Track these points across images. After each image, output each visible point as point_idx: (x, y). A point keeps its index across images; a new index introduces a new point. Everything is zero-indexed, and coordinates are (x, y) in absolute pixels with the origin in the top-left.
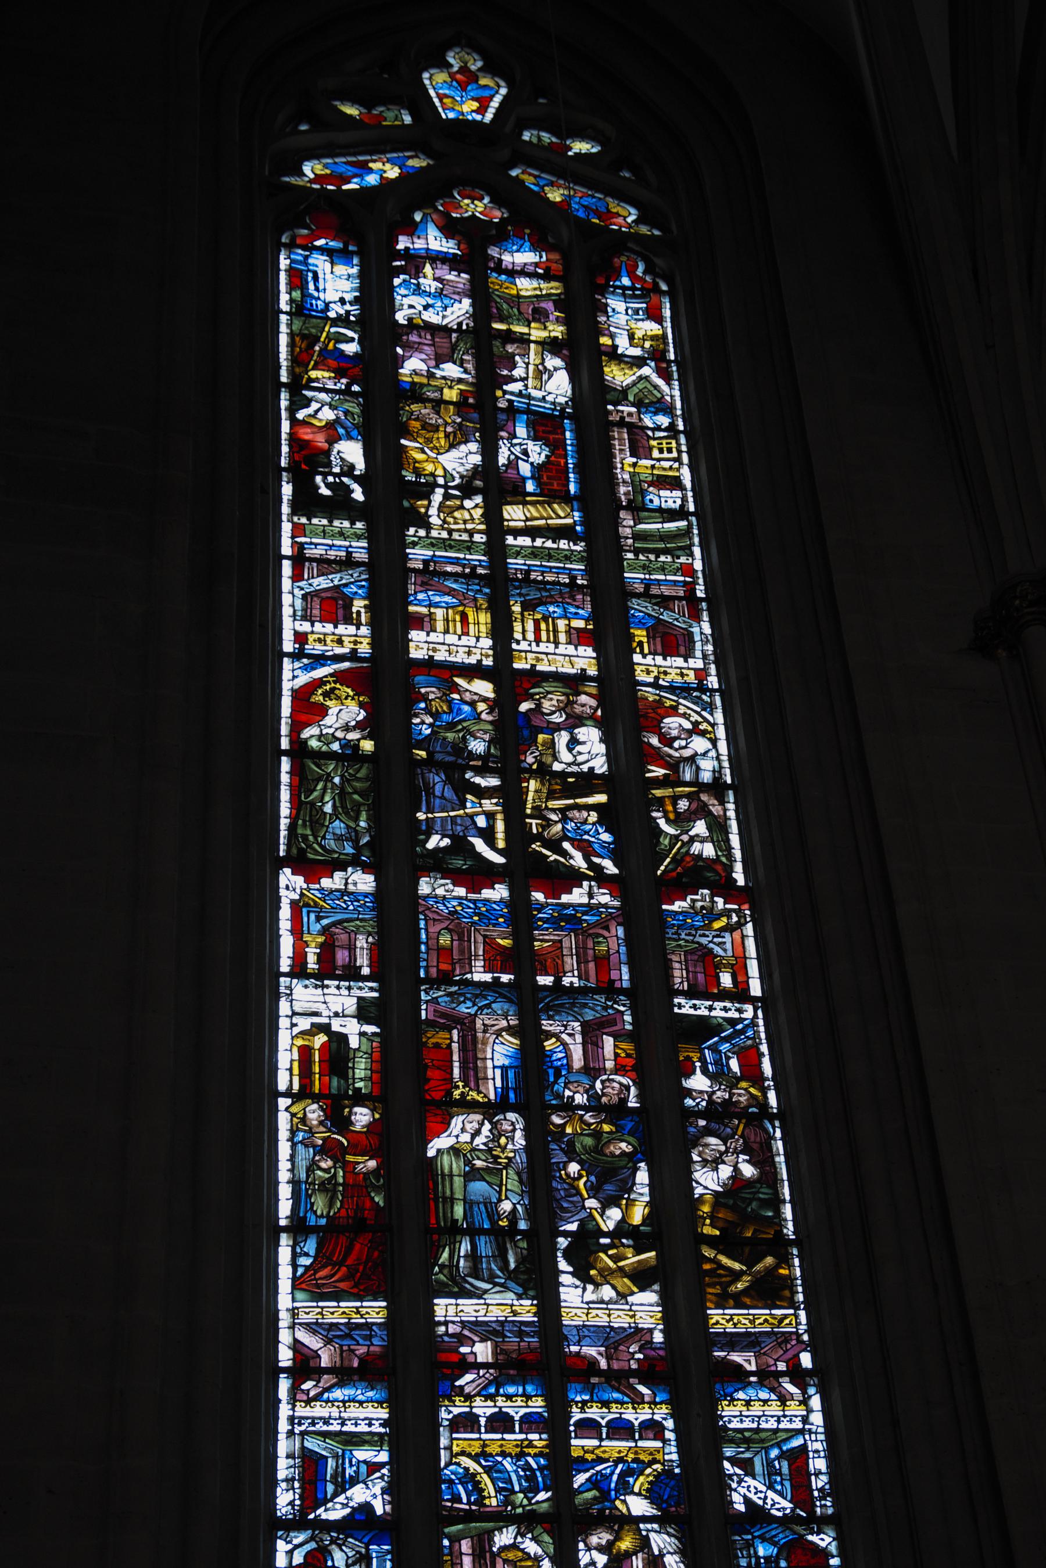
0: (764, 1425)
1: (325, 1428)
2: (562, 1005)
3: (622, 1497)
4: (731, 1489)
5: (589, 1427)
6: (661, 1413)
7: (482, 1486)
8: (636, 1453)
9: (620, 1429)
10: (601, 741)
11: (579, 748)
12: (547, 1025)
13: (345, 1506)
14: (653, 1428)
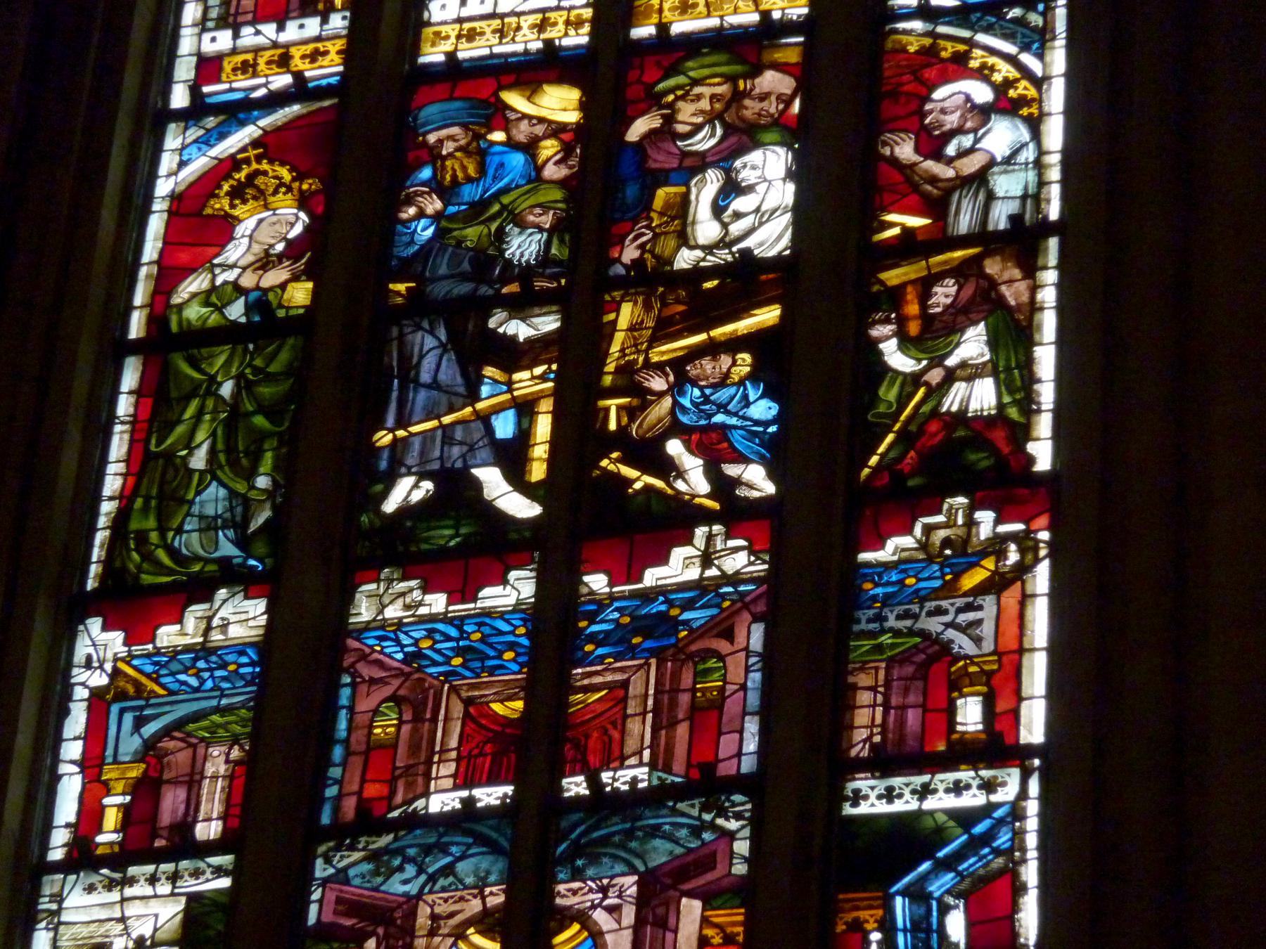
2: (605, 841)
10: (790, 175)
11: (740, 204)
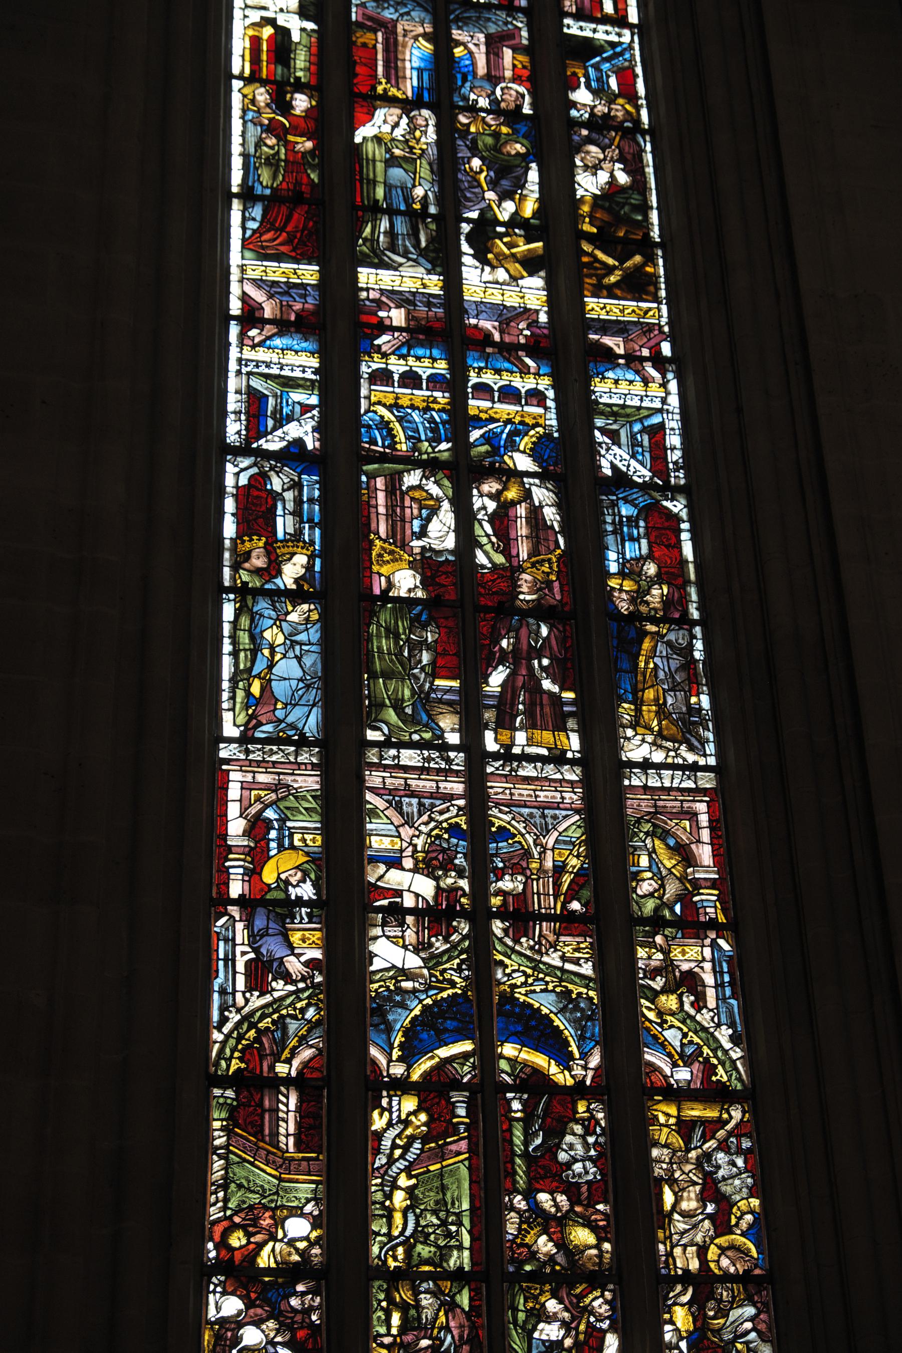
0: (628, 403)
1: (266, 371)
2: (469, 18)
3: (510, 454)
4: (600, 456)
5: (483, 390)
6: (544, 383)
7: (395, 432)
8: (522, 416)
9: (509, 394)
12: (456, 34)
13: (282, 439)
14: (536, 396)
